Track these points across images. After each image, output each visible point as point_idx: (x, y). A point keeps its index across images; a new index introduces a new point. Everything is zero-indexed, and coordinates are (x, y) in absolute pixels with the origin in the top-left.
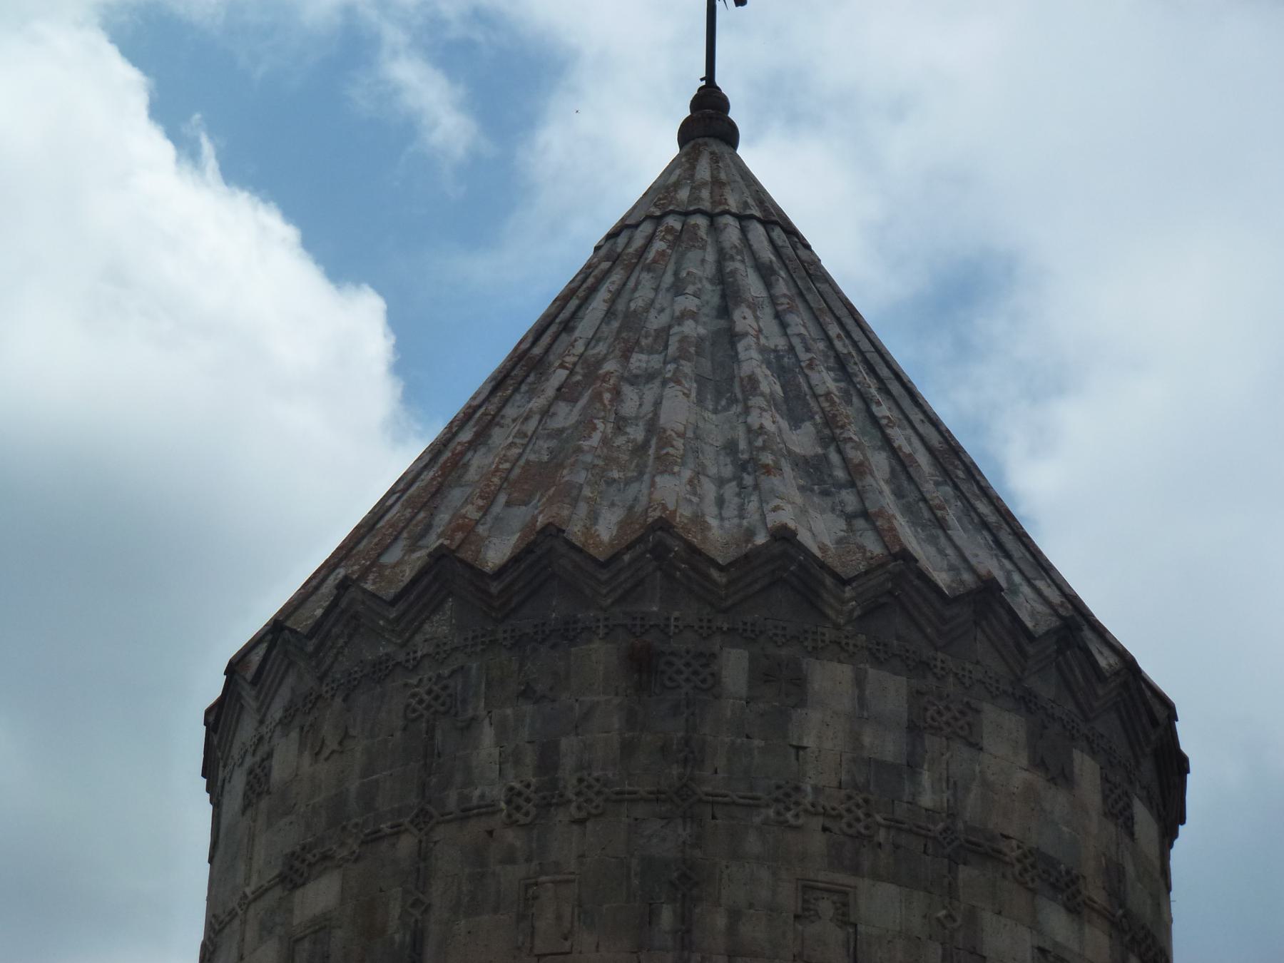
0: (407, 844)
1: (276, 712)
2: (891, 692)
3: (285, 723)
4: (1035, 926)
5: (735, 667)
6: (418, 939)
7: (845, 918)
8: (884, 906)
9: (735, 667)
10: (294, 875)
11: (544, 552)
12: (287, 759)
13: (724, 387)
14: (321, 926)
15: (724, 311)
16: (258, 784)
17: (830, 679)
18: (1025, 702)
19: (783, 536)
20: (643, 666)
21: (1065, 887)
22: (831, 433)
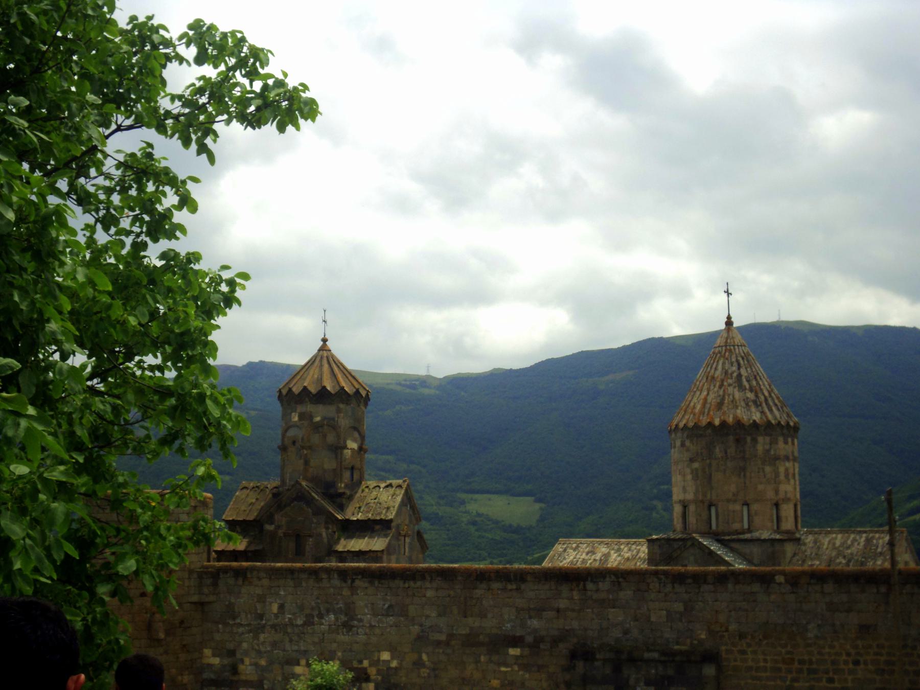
0: (708, 461)
1: (685, 435)
2: (768, 439)
3: (688, 437)
5: (749, 439)
6: (711, 475)
7: (764, 471)
8: (768, 469)
9: (749, 439)
10: (692, 460)
11: (724, 424)
12: (688, 443)
13: (741, 387)
14: (697, 469)
15: (739, 369)
16: (683, 445)
17: (760, 439)
18: (783, 435)
19: (754, 421)
20: (738, 441)
21: (787, 458)
22: (757, 396)
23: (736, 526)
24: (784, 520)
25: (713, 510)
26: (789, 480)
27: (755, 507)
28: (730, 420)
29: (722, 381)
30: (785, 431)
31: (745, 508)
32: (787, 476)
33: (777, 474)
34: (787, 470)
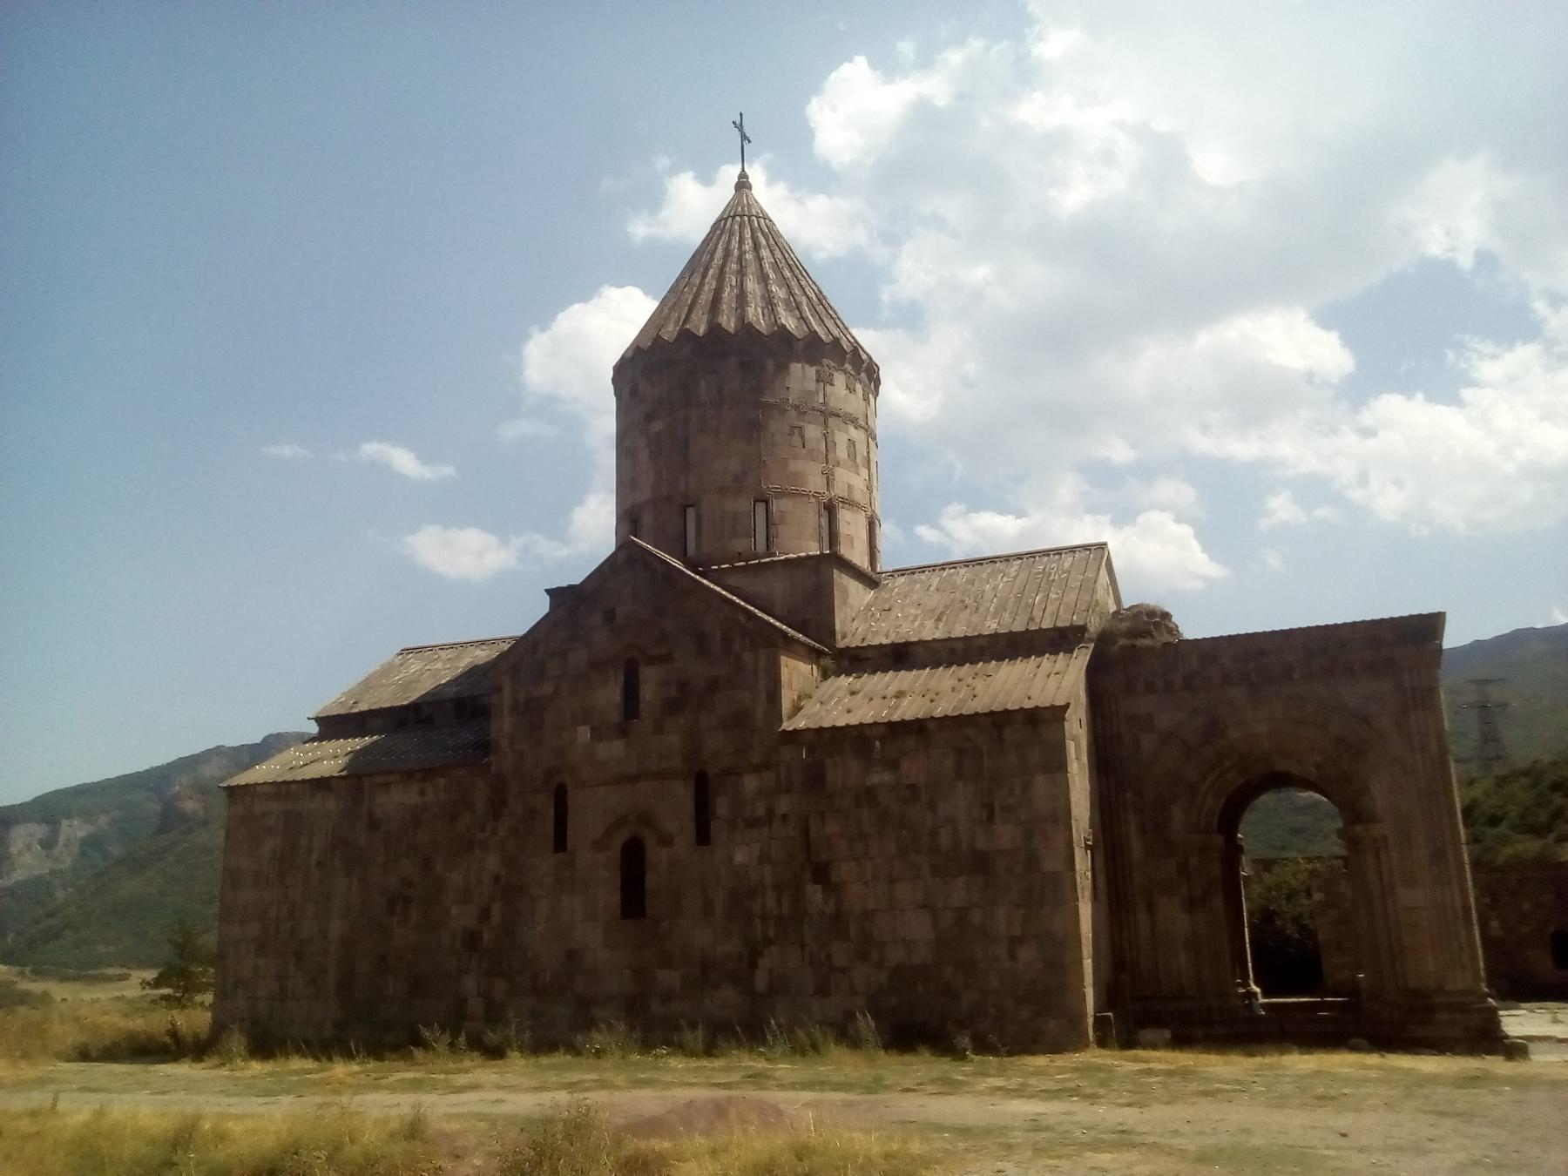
2: (811, 371)
4: (847, 432)
5: (770, 365)
10: (649, 418)
16: (634, 392)
17: (796, 368)
18: (845, 372)
21: (854, 421)
23: (739, 545)
24: (842, 539)
25: (691, 513)
26: (857, 466)
27: (776, 505)
28: (728, 322)
29: (724, 265)
30: (848, 366)
31: (761, 508)
32: (852, 455)
33: (830, 445)
34: (852, 443)
